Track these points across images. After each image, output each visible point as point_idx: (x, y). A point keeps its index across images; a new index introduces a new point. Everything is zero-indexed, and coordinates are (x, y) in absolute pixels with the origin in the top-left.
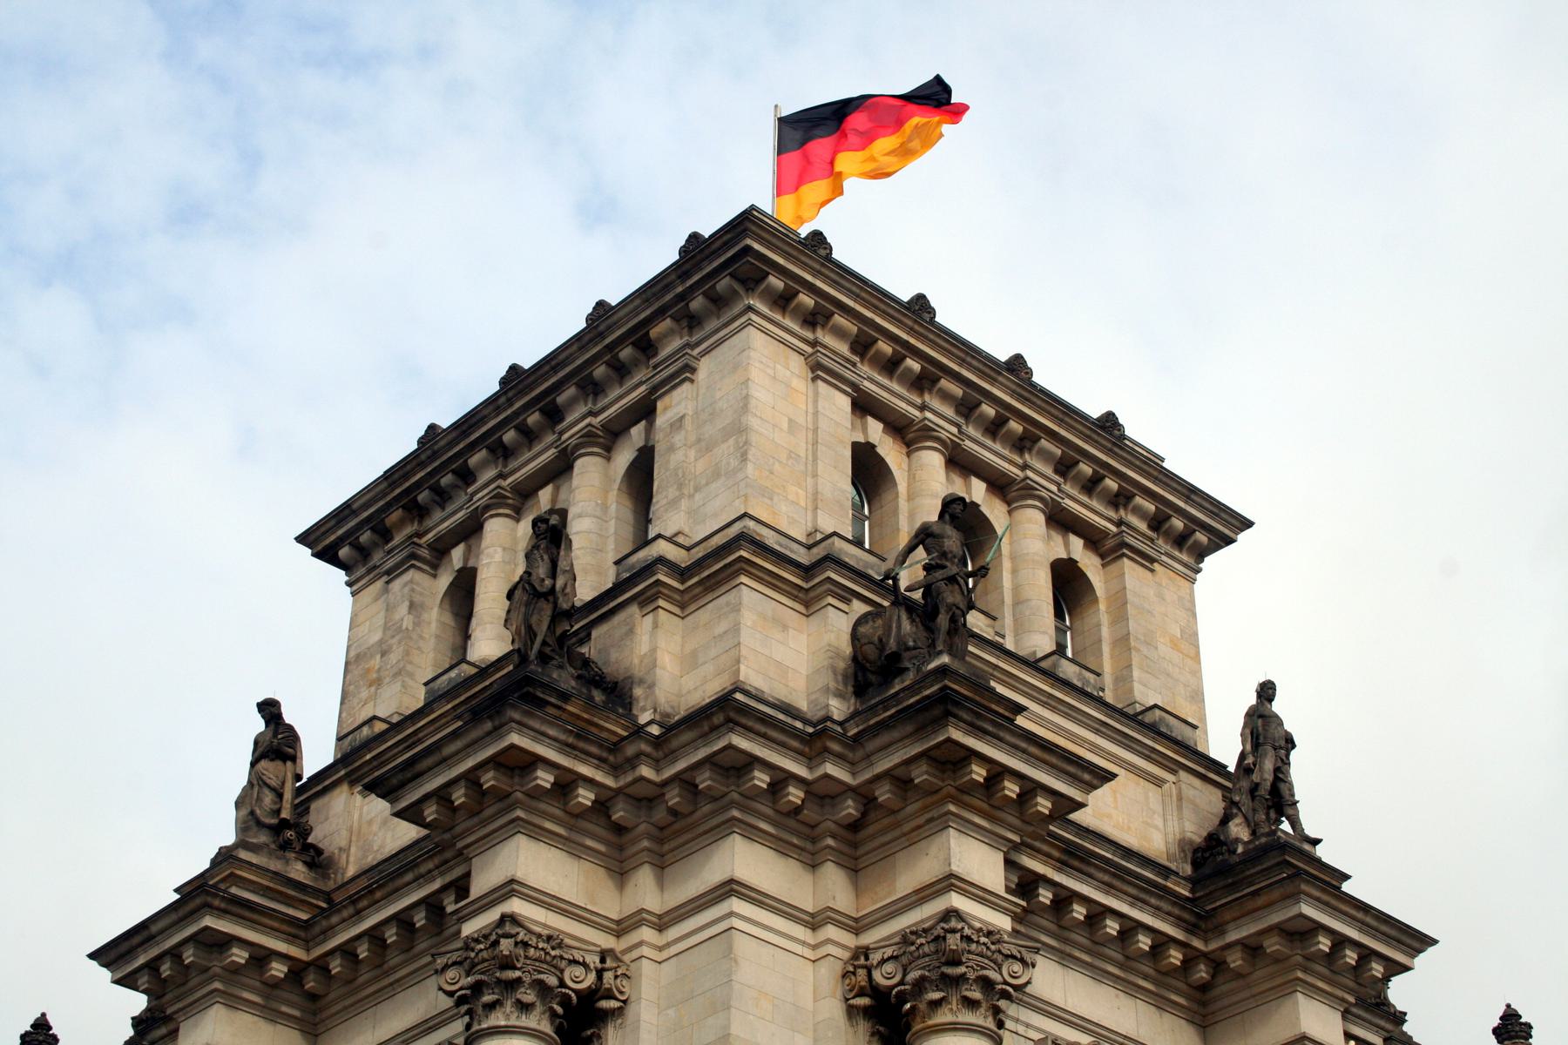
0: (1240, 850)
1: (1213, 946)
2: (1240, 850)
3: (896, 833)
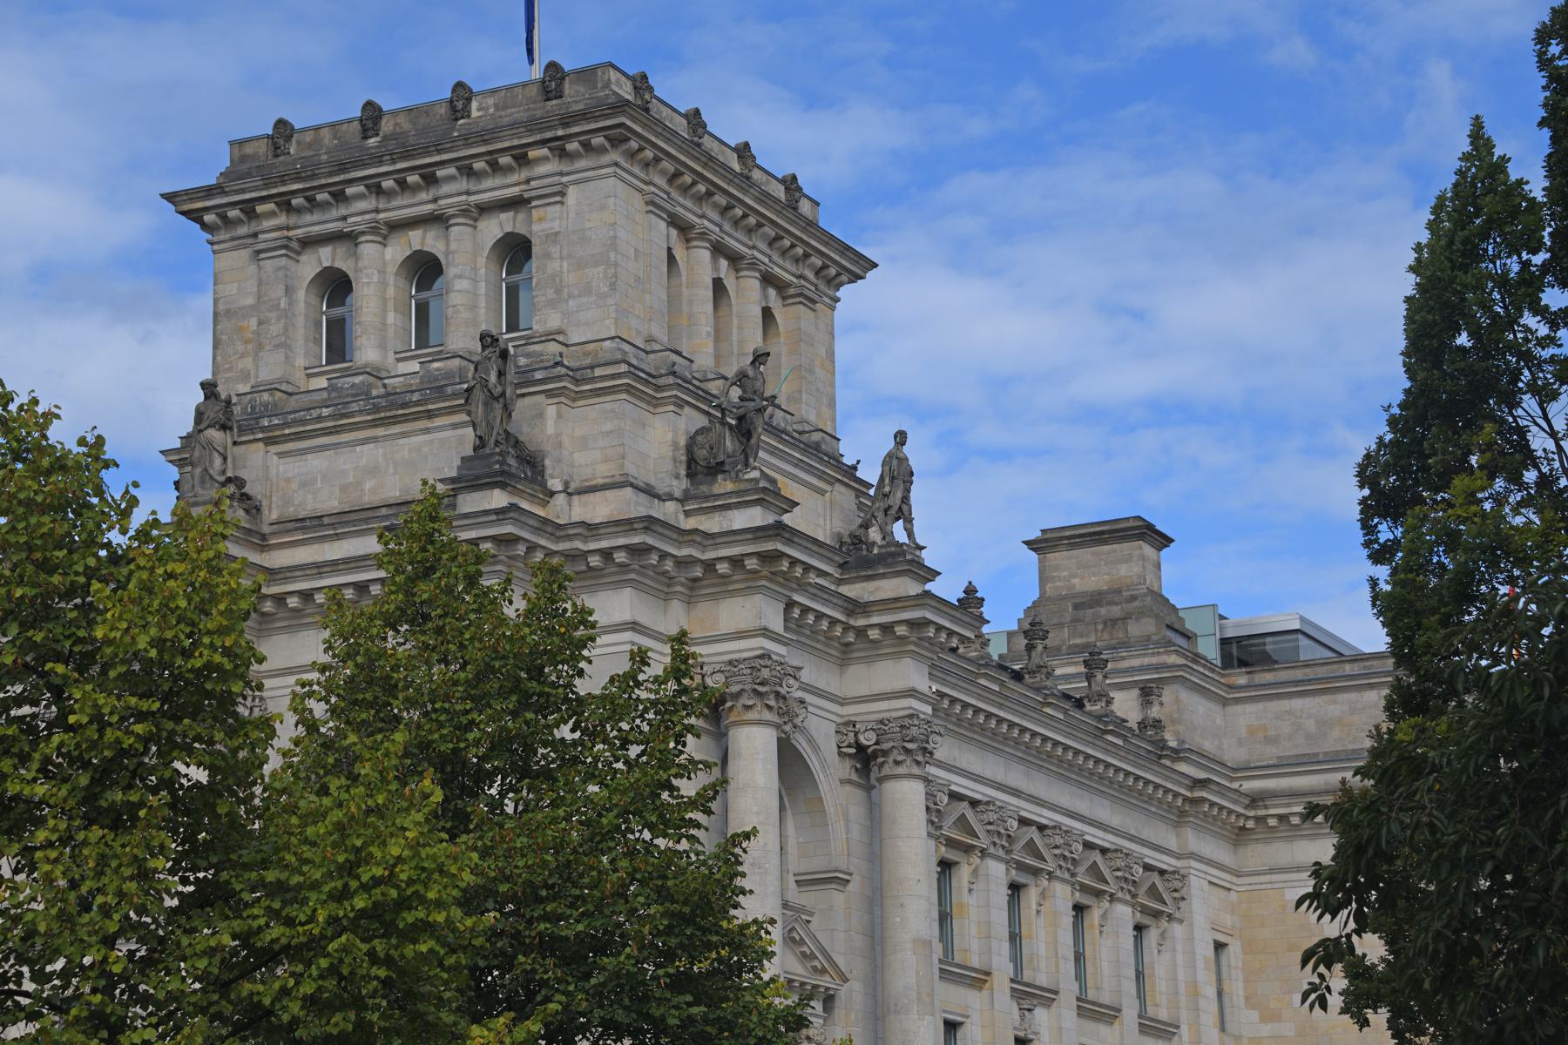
0: (876, 551)
1: (861, 622)
2: (876, 551)
3: (724, 588)
